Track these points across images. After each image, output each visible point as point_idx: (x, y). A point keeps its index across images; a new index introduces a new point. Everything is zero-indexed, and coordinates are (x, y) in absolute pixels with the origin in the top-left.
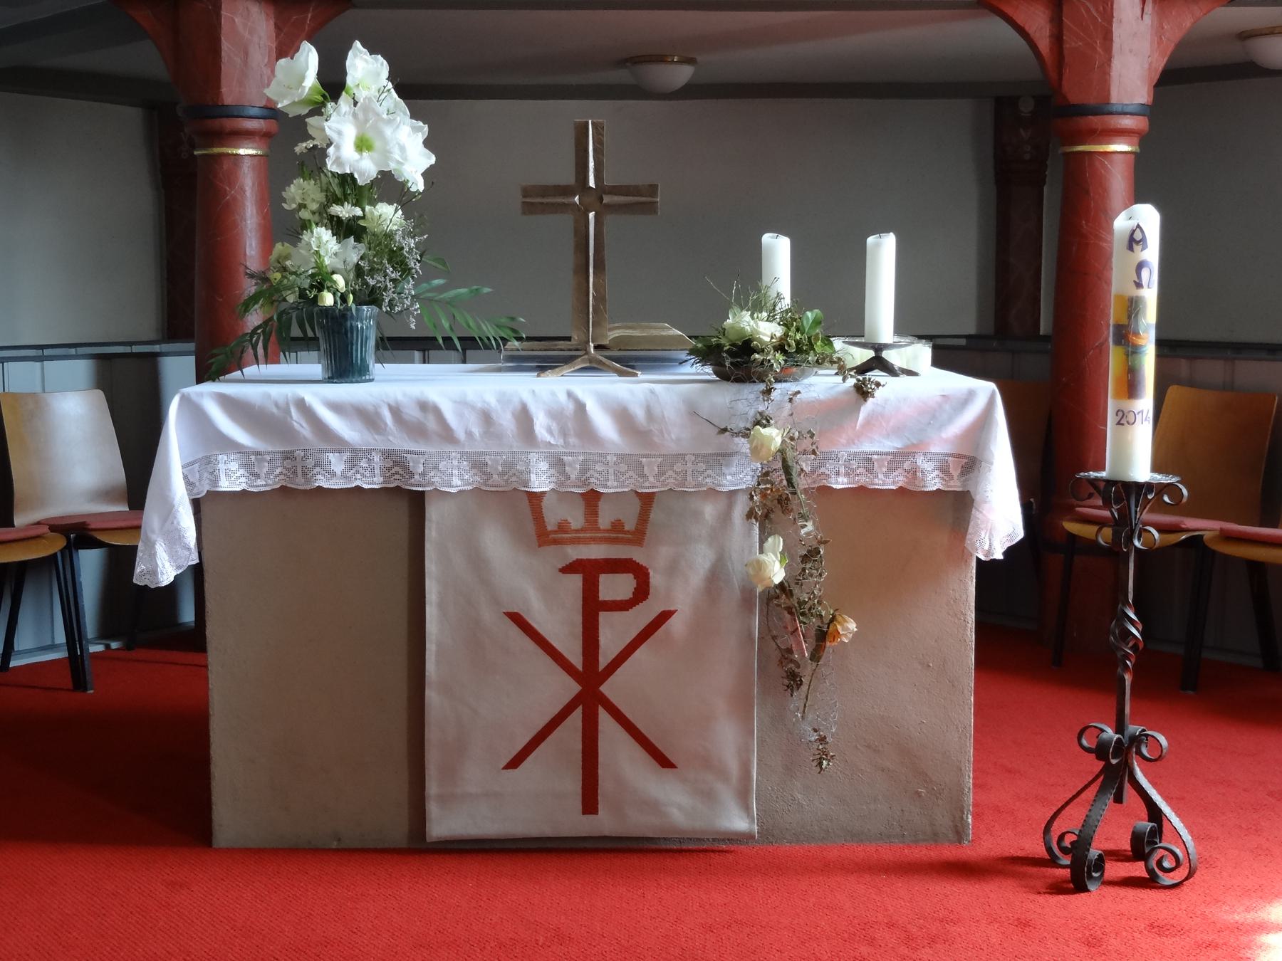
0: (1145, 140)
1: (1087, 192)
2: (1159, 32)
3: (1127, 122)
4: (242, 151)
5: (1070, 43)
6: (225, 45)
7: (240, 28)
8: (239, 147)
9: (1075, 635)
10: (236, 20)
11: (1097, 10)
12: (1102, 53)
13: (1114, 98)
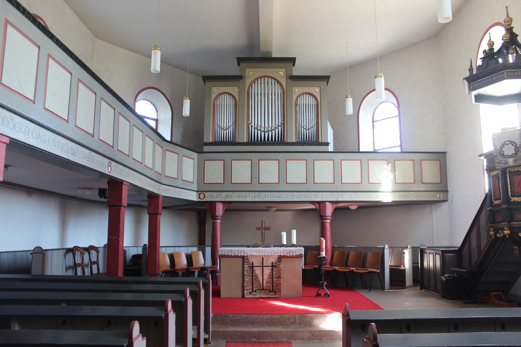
0: (331, 220)
2: (332, 207)
3: (329, 218)
4: (218, 221)
6: (217, 208)
13: (327, 215)
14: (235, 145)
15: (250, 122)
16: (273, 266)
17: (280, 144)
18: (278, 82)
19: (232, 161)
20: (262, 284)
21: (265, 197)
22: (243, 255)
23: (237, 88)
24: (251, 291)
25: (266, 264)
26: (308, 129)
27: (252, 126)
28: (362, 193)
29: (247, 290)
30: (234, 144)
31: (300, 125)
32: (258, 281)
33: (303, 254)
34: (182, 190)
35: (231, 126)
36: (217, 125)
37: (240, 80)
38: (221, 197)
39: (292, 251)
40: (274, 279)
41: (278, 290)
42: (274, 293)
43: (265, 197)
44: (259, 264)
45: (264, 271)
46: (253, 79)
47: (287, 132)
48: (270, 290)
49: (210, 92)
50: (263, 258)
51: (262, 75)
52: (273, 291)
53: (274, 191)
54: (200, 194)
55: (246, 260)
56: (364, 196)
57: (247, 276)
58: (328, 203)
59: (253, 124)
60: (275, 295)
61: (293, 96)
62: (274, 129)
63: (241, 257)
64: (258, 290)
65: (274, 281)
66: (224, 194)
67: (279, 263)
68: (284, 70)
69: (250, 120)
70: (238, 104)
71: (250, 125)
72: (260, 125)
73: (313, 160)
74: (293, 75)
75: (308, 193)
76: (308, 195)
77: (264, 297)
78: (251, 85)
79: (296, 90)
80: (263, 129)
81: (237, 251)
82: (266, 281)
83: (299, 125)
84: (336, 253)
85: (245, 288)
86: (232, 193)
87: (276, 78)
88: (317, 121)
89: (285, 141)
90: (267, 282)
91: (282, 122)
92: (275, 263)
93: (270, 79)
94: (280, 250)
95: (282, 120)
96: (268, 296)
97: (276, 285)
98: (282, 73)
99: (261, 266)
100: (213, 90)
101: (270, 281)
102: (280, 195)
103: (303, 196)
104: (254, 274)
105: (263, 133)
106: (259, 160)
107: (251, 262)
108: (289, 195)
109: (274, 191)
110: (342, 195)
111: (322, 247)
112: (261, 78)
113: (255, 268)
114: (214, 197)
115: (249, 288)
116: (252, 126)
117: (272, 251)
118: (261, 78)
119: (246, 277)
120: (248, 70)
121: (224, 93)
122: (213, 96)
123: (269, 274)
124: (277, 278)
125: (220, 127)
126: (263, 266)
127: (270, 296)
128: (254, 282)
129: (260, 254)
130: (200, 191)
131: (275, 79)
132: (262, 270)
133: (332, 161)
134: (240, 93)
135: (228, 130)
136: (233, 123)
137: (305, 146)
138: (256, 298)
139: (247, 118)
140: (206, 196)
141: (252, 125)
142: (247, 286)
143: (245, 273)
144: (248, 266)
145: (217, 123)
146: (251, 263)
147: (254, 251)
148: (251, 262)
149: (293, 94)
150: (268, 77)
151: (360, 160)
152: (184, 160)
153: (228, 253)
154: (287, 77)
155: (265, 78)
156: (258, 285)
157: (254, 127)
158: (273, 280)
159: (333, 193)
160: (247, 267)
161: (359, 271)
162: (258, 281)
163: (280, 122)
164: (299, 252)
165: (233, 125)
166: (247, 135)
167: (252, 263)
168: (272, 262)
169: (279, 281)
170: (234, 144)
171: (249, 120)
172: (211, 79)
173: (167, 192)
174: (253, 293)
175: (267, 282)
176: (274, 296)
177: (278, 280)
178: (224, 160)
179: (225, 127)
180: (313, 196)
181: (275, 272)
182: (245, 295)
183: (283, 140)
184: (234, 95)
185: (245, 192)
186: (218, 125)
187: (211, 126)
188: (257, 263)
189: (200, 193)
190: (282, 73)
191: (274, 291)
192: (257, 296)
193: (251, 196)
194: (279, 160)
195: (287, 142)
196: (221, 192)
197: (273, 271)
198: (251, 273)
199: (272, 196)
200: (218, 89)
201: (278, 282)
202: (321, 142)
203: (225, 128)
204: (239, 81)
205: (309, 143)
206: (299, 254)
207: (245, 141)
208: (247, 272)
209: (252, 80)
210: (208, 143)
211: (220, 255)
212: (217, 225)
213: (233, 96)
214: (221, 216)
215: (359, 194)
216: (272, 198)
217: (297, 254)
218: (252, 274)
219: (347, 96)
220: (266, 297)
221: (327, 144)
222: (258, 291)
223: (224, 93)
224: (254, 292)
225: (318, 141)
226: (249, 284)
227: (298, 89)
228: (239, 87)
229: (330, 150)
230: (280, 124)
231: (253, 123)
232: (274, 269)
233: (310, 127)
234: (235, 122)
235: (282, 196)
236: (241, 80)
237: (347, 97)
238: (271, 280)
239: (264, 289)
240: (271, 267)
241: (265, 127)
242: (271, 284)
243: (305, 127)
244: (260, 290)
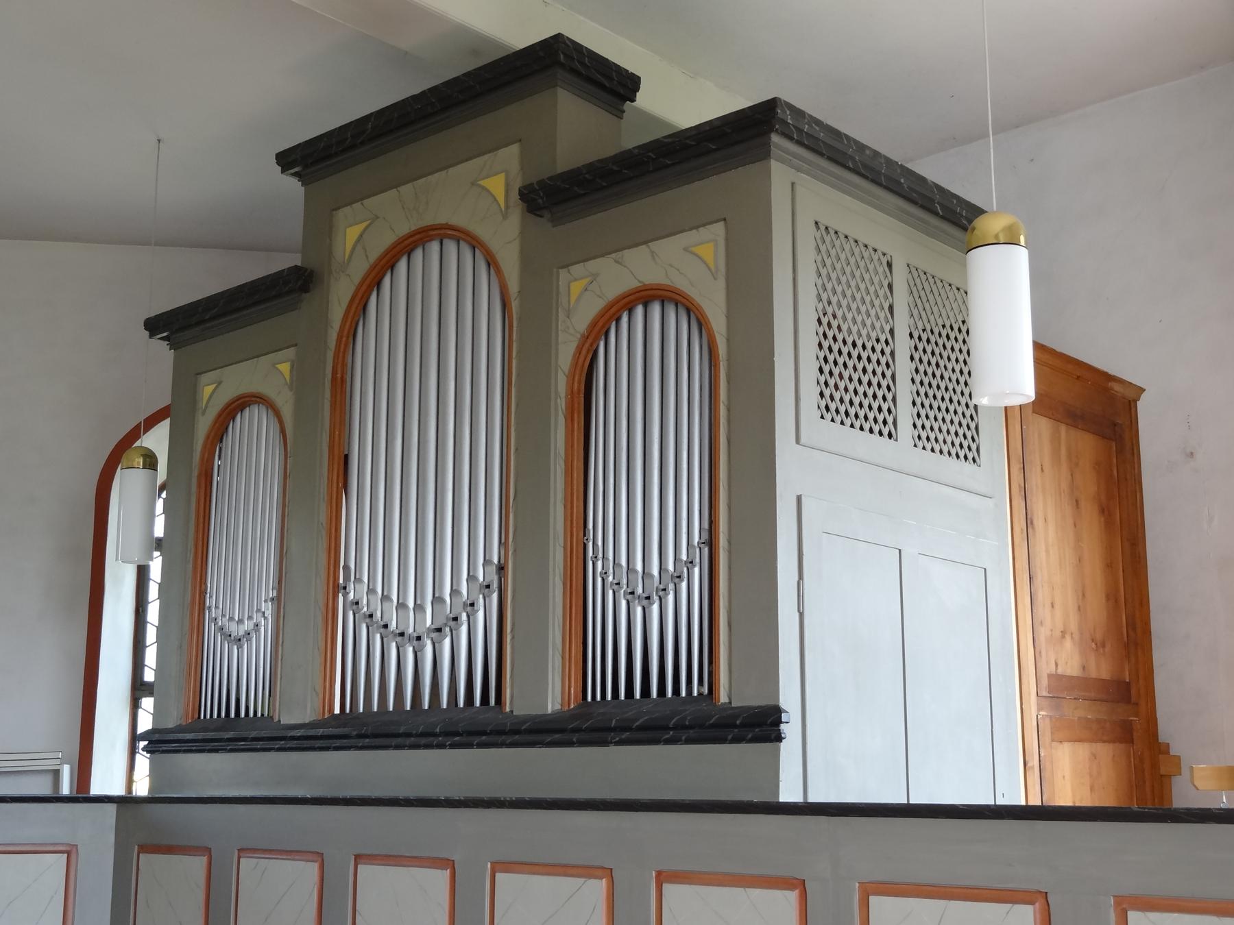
46: (359, 269)
79: (576, 288)
83: (599, 564)
93: (451, 247)
133: (792, 896)
134: (301, 382)
137: (612, 749)
178: (207, 851)
190: (496, 185)
200: (220, 383)
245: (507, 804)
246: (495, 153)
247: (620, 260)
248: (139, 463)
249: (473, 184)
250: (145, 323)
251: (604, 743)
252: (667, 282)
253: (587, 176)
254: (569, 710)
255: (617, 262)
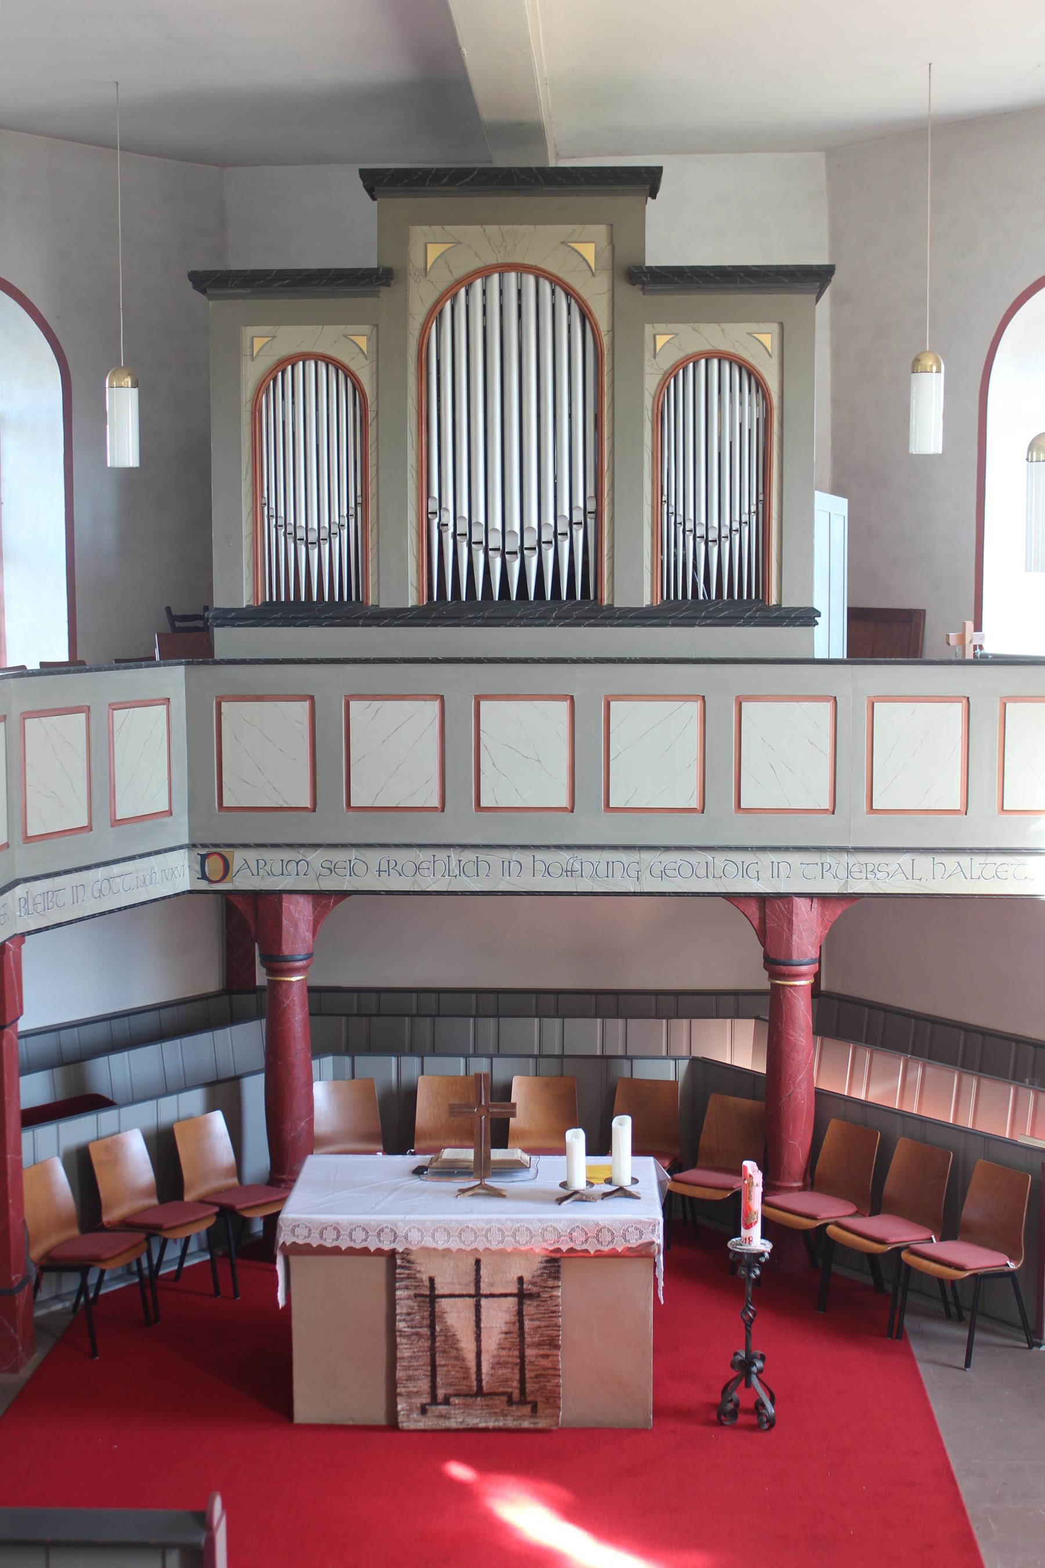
1: (781, 1007)
2: (823, 916)
3: (804, 969)
4: (294, 979)
5: (771, 924)
6: (285, 922)
7: (293, 911)
8: (292, 977)
9: (776, 1261)
10: (291, 907)
11: (784, 907)
12: (787, 931)
14: (361, 622)
15: (433, 506)
16: (522, 1296)
17: (577, 618)
18: (570, 293)
19: (353, 704)
20: (473, 1370)
21: (506, 873)
22: (387, 1246)
23: (366, 328)
24: (428, 1400)
25: (492, 1285)
26: (719, 540)
27: (442, 526)
28: (965, 860)
29: (409, 1395)
30: (359, 618)
31: (680, 519)
32: (457, 1358)
33: (660, 1241)
34: (115, 869)
35: (340, 526)
36: (273, 522)
37: (382, 288)
38: (301, 873)
39: (609, 1230)
40: (530, 1352)
41: (547, 1398)
42: (527, 1409)
43: (506, 873)
44: (460, 1284)
45: (483, 1317)
46: (444, 281)
47: (612, 558)
48: (510, 1396)
49: (234, 353)
50: (478, 1262)
51: (491, 260)
52: (523, 1402)
53: (548, 847)
54: (204, 858)
55: (401, 1267)
56: (976, 873)
57: (409, 1336)
58: (802, 906)
59: (448, 518)
60: (533, 1420)
61: (647, 369)
62: (551, 538)
63: (379, 1252)
64: (457, 1395)
65: (527, 1360)
66: (316, 857)
67: (550, 1283)
68: (602, 229)
69: (436, 494)
70: (371, 415)
71: (436, 521)
72: (482, 520)
73: (737, 697)
74: (647, 264)
75: (708, 856)
76: (711, 865)
77: (482, 1425)
78: (435, 314)
79: (661, 341)
80: (495, 541)
81: (364, 1229)
82: (494, 1357)
84: (833, 1128)
85: (399, 1390)
86: (353, 853)
87: (561, 275)
88: (761, 497)
89: (605, 603)
90: (497, 1364)
91: (591, 506)
92: (534, 1284)
94: (555, 1229)
95: (591, 492)
96: (500, 1424)
97: (537, 1376)
98: (588, 251)
99: (470, 1296)
100: (246, 343)
101: (510, 1360)
102: (577, 866)
103: (686, 871)
104: (438, 1328)
105: (498, 561)
106: (478, 699)
107: (425, 1277)
108: (618, 867)
109: (548, 847)
110: (870, 868)
111: (750, 1209)
112: (485, 273)
113: (444, 1304)
114: (271, 874)
115: (415, 1390)
116: (442, 526)
117: (518, 1230)
118: (485, 273)
119: (404, 1341)
120: (418, 233)
121: (305, 357)
122: (252, 373)
123: (504, 1329)
124: (539, 1345)
125: (290, 529)
126: (478, 1295)
127: (510, 1423)
128: (439, 1361)
129: (464, 1242)
130: (204, 846)
131: (556, 282)
132: (473, 1310)
133: (828, 706)
135: (327, 545)
136: (352, 512)
137: (696, 628)
138: (448, 1430)
139: (419, 488)
140: (235, 866)
141: (444, 521)
142: (409, 1378)
143: (401, 1325)
144: (412, 1293)
145: (273, 512)
146: (427, 1283)
147: (436, 1230)
148: (425, 1277)
149: (646, 362)
150: (522, 269)
151: (965, 701)
152: (116, 728)
153: (321, 1237)
154: (613, 270)
155: (506, 274)
156: (461, 1375)
157: (451, 530)
158: (522, 1356)
159: (828, 858)
160: (409, 1298)
161: (926, 1263)
162: (457, 1358)
163: (581, 505)
164: (641, 1233)
165: (352, 521)
166: (419, 572)
167: (432, 1280)
168: (520, 1280)
169: (551, 1358)
170: (359, 618)
171: (429, 495)
172: (238, 286)
173: (40, 908)
174: (433, 1408)
175: (498, 1363)
176: (526, 1424)
177: (547, 1356)
179: (313, 529)
180: (731, 869)
181: (532, 1320)
182: (400, 1419)
183: (592, 598)
184: (353, 366)
185: (417, 850)
186: (281, 522)
187: (246, 528)
188: (452, 1283)
189: (204, 852)
190: (588, 251)
191: (529, 1399)
192: (453, 1424)
193: (440, 866)
194: (572, 698)
195: (611, 607)
196: (302, 850)
197: (525, 1318)
198: (426, 1322)
199: (540, 867)
200: (274, 337)
201: (545, 1362)
202: (778, 607)
203: (313, 537)
204: (376, 294)
205: (722, 610)
206: (640, 1242)
207: (412, 601)
208: (408, 1318)
209: (442, 287)
210: (233, 614)
211: (288, 1244)
212: (287, 998)
213: (349, 374)
214: (309, 956)
215: (950, 861)
216: (539, 877)
217: (634, 1243)
218: (432, 1326)
219: (917, 360)
220: (491, 1425)
221: (807, 617)
222: (457, 1402)
223: (305, 357)
224: (440, 1404)
225: (763, 601)
226: (416, 1373)
227: (672, 336)
228: (376, 325)
229: (818, 655)
230: (578, 516)
231: (447, 510)
232: (530, 1308)
233: (725, 532)
234: (363, 503)
235: (588, 869)
236: (389, 288)
237: (916, 366)
238: (517, 1353)
239: (485, 1389)
240: (512, 1302)
241: (507, 529)
242: (517, 1371)
243: (701, 531)
244: (466, 1395)
245: (657, 661)
246: (583, 226)
247: (697, 329)
248: (128, 384)
249: (562, 243)
250: (188, 276)
251: (693, 625)
252: (736, 353)
253: (689, 274)
254: (658, 606)
255: (693, 328)
